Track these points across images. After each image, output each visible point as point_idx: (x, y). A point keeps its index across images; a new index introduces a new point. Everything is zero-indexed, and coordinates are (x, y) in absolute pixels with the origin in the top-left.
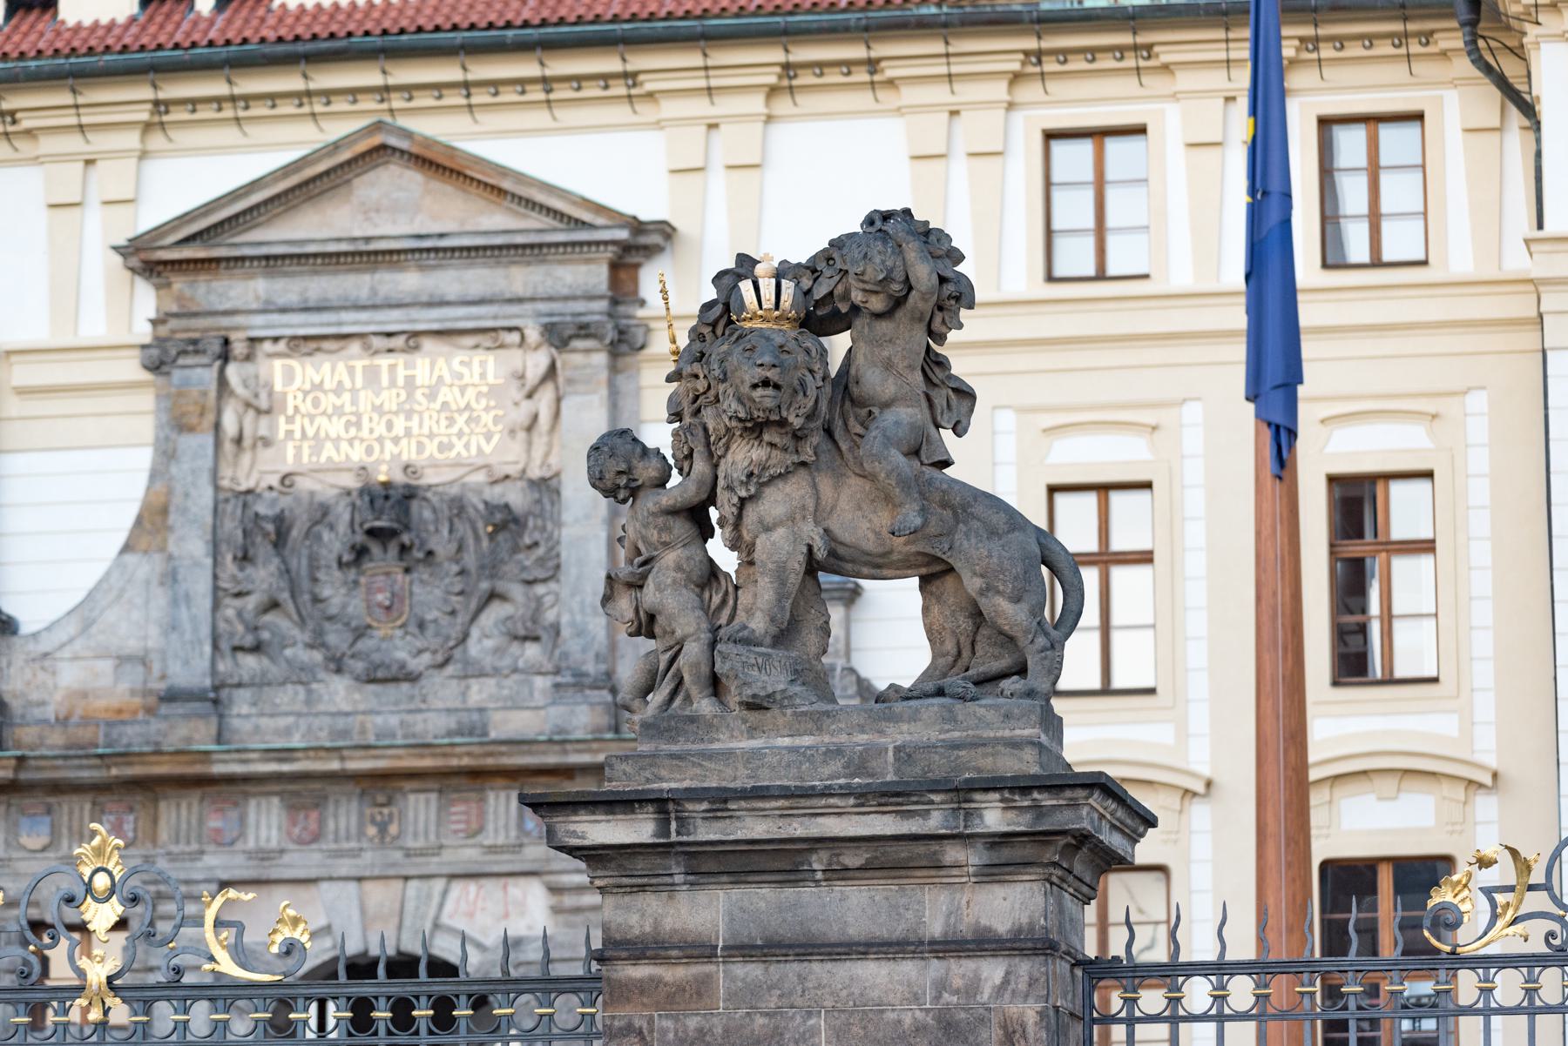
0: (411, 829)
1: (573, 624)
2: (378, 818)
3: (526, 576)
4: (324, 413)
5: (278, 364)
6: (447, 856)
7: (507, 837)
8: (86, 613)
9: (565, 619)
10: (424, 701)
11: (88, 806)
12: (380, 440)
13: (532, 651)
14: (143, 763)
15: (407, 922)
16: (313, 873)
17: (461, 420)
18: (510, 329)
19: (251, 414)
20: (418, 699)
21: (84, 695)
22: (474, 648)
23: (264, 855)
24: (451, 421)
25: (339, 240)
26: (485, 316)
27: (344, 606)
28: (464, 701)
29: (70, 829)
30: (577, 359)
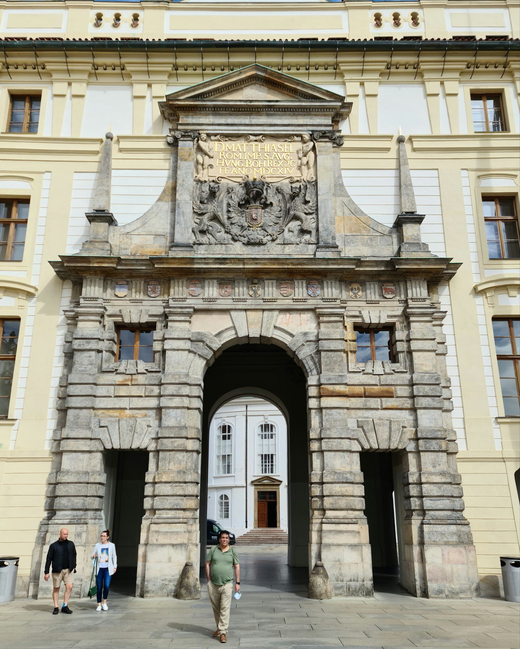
1: (323, 227)
6: (279, 302)
8: (144, 219)
10: (269, 252)
11: (143, 282)
13: (307, 237)
14: (168, 263)
15: (264, 326)
16: (229, 307)
17: (280, 164)
18: (297, 136)
19: (207, 157)
20: (266, 251)
21: (142, 247)
22: (286, 234)
25: (241, 101)
26: (290, 130)
27: (239, 220)
30: (323, 144)
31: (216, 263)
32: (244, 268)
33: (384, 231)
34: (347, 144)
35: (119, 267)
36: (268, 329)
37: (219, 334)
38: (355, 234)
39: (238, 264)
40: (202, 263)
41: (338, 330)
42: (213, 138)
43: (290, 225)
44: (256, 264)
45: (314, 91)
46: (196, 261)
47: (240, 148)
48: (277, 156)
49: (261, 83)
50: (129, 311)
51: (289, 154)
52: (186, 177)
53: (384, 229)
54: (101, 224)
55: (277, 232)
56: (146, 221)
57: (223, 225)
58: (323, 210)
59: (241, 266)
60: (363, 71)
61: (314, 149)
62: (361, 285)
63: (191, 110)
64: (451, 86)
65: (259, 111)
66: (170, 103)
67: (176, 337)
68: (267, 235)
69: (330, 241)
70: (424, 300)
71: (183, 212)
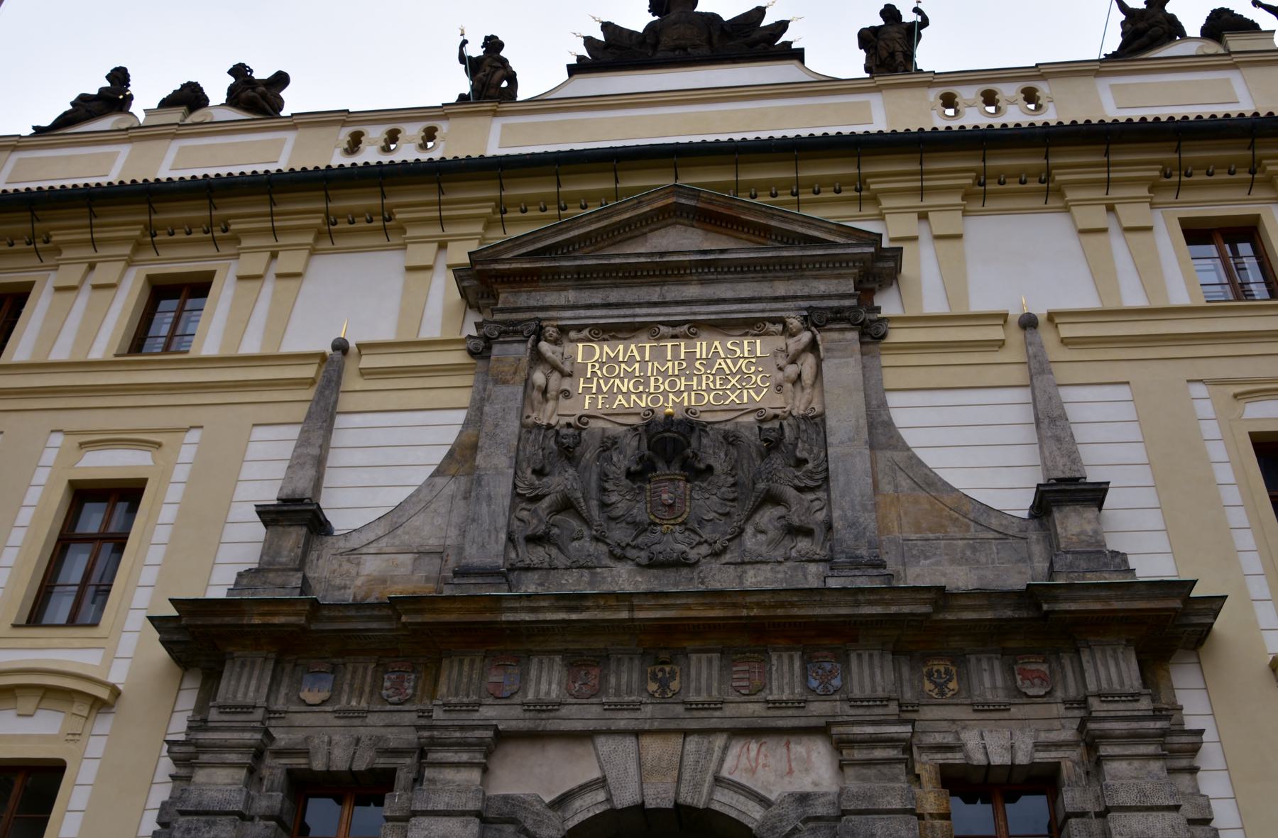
0: (693, 685)
2: (660, 675)
3: (797, 482)
4: (618, 376)
5: (580, 345)
6: (729, 710)
7: (793, 693)
8: (395, 519)
9: (836, 514)
12: (665, 393)
13: (803, 544)
14: (434, 611)
15: (687, 776)
16: (591, 725)
18: (774, 321)
21: (384, 581)
22: (750, 541)
23: (543, 707)
24: (726, 381)
26: (755, 310)
27: (629, 509)
28: (741, 583)
29: (351, 686)
30: (835, 335)
31: (558, 609)
32: (632, 620)
33: (1006, 527)
34: (897, 335)
35: (313, 627)
36: (697, 786)
37: (562, 802)
38: (931, 536)
39: (618, 609)
40: (523, 609)
41: (897, 785)
42: (573, 334)
43: (757, 518)
44: (665, 607)
45: (809, 228)
46: (505, 604)
47: (636, 353)
48: (724, 366)
49: (686, 222)
50: (326, 739)
51: (754, 360)
52: (504, 419)
53: (1004, 522)
54: (292, 529)
55: (724, 534)
56: (400, 521)
57: (586, 522)
58: (842, 479)
59: (624, 615)
60: (922, 192)
61: (813, 346)
62: (953, 663)
63: (526, 281)
64: (1133, 214)
65: (682, 275)
66: (478, 267)
67: (441, 807)
68: (700, 543)
69: (864, 552)
70: (1135, 697)
71: (489, 496)
